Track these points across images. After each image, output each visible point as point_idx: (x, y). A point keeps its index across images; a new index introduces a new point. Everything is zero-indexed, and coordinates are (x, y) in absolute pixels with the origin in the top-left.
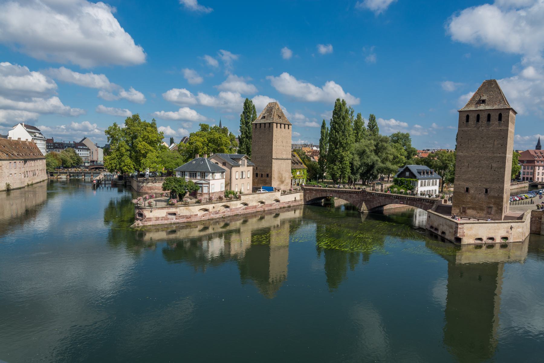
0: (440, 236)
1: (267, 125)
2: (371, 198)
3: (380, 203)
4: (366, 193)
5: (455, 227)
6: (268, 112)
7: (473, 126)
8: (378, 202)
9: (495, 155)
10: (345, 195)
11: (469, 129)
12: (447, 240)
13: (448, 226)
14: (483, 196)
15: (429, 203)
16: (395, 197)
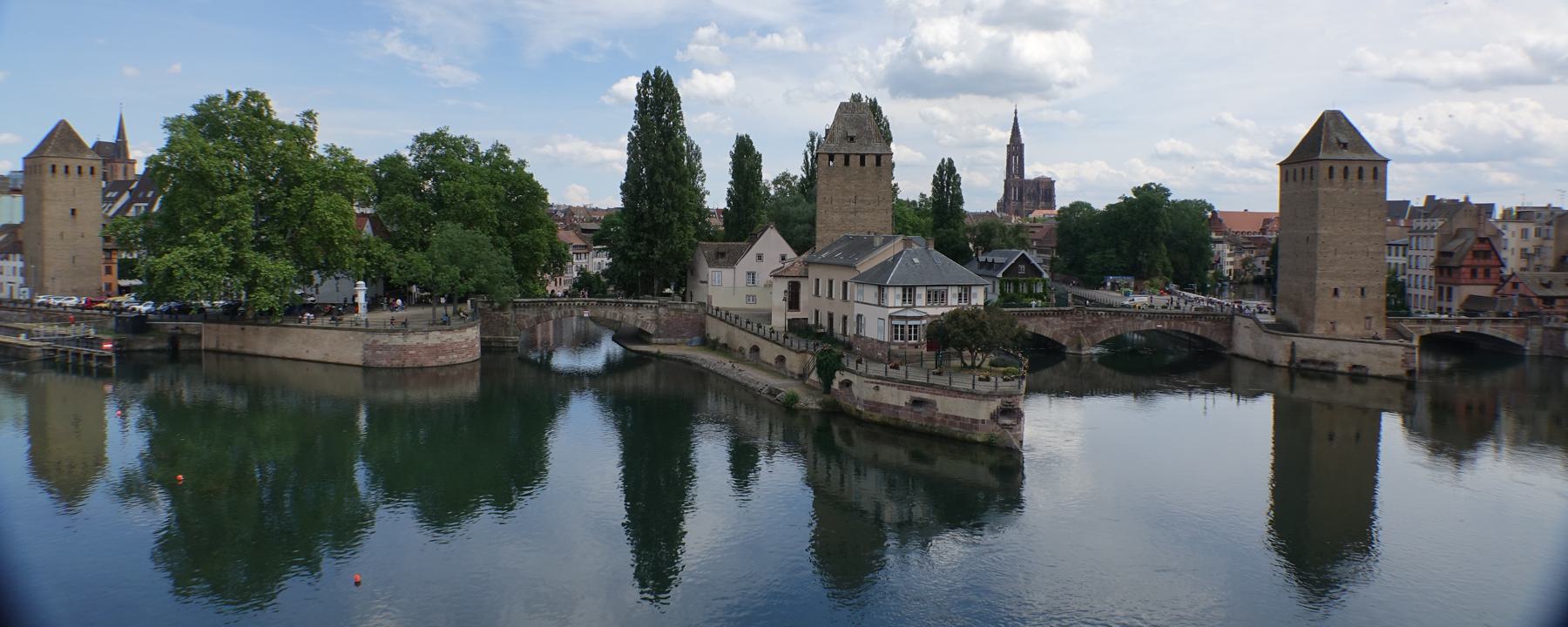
0: (1342, 373)
1: (871, 161)
2: (1094, 322)
3: (1114, 330)
4: (1086, 313)
5: (1403, 353)
6: (856, 127)
7: (1340, 185)
8: (1111, 330)
9: (1371, 234)
10: (1032, 320)
11: (1335, 190)
12: (1379, 377)
13: (1374, 354)
14: (1358, 300)
15: (1210, 323)
16: (1147, 315)
